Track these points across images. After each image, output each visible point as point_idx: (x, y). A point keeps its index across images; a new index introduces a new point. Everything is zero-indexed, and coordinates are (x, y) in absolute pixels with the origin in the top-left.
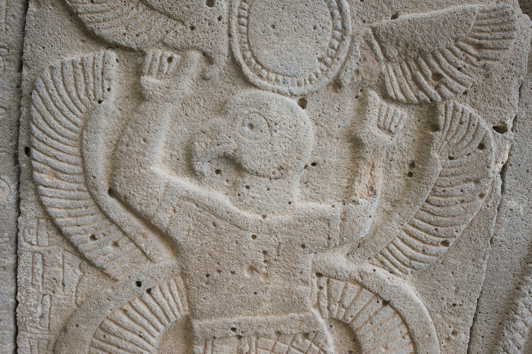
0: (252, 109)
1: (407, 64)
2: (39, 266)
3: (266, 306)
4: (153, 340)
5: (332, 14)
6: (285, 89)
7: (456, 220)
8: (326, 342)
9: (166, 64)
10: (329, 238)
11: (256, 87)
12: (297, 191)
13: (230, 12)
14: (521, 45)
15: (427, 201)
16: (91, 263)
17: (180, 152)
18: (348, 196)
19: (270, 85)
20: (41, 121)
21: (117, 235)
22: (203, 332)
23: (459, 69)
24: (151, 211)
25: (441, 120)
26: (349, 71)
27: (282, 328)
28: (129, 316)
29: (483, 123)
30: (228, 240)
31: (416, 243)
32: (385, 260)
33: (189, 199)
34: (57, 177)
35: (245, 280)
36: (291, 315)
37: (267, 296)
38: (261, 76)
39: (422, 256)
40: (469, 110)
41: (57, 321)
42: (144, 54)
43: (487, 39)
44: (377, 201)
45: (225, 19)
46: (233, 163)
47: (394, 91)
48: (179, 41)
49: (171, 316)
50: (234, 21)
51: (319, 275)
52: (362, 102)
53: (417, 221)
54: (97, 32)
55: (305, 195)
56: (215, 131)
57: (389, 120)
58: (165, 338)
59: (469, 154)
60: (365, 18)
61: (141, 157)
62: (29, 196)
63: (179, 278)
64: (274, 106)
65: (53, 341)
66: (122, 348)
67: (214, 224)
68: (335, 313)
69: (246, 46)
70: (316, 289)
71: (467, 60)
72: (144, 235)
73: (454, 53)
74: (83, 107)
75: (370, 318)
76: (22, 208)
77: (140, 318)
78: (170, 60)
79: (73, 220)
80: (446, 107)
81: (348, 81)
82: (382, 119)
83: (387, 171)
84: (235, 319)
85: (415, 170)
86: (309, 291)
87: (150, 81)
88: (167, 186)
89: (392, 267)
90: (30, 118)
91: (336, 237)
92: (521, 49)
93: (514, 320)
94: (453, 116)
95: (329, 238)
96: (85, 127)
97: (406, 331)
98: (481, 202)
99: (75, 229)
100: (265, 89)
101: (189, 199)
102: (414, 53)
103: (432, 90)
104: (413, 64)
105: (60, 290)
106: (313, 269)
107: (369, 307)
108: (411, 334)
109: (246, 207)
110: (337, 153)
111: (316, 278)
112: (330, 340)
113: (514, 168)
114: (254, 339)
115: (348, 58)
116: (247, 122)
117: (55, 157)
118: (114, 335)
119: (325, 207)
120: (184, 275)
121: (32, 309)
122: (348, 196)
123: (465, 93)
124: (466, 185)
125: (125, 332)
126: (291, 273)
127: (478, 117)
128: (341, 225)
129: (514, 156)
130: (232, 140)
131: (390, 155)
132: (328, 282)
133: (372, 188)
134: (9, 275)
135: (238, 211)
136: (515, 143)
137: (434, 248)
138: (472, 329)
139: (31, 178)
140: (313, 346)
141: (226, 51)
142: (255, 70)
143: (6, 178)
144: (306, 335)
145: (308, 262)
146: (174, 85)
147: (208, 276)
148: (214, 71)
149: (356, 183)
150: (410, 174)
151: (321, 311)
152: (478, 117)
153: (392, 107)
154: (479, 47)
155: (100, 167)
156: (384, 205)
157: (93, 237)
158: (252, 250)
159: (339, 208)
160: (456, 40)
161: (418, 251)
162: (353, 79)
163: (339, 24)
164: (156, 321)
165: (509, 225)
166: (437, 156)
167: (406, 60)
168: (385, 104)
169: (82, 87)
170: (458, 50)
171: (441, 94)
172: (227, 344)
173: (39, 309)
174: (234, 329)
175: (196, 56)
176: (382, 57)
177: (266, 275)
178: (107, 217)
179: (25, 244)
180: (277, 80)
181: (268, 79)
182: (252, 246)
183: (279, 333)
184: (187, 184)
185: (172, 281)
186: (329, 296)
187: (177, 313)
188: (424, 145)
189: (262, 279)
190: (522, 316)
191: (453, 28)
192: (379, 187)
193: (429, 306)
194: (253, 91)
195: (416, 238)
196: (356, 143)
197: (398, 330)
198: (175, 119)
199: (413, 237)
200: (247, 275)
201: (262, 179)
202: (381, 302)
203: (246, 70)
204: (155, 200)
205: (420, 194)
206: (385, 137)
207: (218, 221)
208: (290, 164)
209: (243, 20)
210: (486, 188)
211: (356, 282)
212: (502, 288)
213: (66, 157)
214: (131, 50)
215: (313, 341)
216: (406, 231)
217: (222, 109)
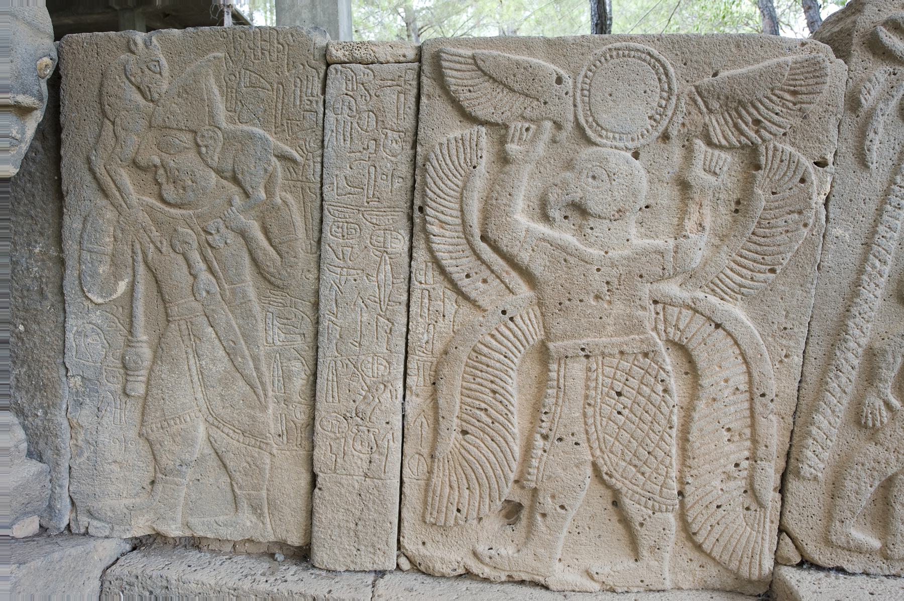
0: (594, 163)
1: (729, 114)
2: (426, 301)
3: (610, 329)
4: (515, 360)
5: (659, 79)
6: (621, 144)
7: (781, 249)
8: (664, 361)
9: (525, 134)
10: (664, 269)
11: (597, 145)
12: (633, 230)
13: (575, 87)
14: (836, 87)
15: (753, 233)
16: (466, 297)
17: (536, 203)
18: (679, 232)
19: (609, 143)
20: (433, 185)
21: (486, 273)
22: (557, 352)
23: (777, 114)
24: (515, 251)
25: (763, 160)
26: (676, 124)
27: (625, 348)
28: (496, 340)
29: (803, 159)
30: (577, 273)
31: (744, 271)
32: (716, 288)
33: (544, 240)
34: (442, 228)
35: (591, 306)
36: (632, 336)
37: (611, 321)
38: (601, 136)
39: (751, 283)
40: (789, 148)
41: (439, 346)
42: (506, 127)
43: (801, 86)
45: (571, 94)
46: (580, 209)
47: (717, 136)
48: (534, 115)
49: (530, 339)
50: (578, 94)
51: (656, 302)
52: (689, 150)
53: (745, 252)
54: (473, 114)
55: (641, 233)
56: (565, 184)
57: (713, 164)
58: (523, 361)
59: (790, 189)
60: (688, 78)
61: (507, 208)
62: (420, 244)
63: (536, 308)
64: (613, 160)
65: (435, 363)
66: (492, 367)
67: (565, 260)
68: (671, 335)
69: (589, 113)
70: (654, 315)
71: (783, 105)
72: (507, 273)
73: (771, 101)
74: (462, 172)
75: (704, 340)
76: (414, 255)
77: (506, 341)
78: (527, 129)
79: (454, 262)
80: (766, 148)
81: (676, 133)
82: (707, 163)
83: (715, 209)
84: (584, 341)
85: (740, 207)
86: (648, 316)
87: (513, 148)
88: (527, 231)
89: (723, 294)
90: (425, 184)
91: (669, 267)
92: (836, 90)
93: (845, 341)
94: (774, 156)
95: (664, 269)
96: (464, 187)
97: (738, 352)
98: (805, 232)
99: (456, 269)
100: (604, 146)
101: (544, 240)
102: (735, 103)
103: (752, 134)
104: (734, 113)
105: (441, 319)
106: (650, 296)
107: (702, 329)
108: (743, 355)
109: (591, 245)
110: (668, 196)
111: (652, 307)
112: (668, 360)
113: (837, 198)
114: (600, 358)
115: (674, 114)
116: (591, 174)
117: (442, 213)
118: (485, 356)
119: (659, 243)
120: (540, 304)
121: (420, 336)
122: (679, 232)
123: (785, 134)
124: (790, 216)
125: (493, 353)
126: (631, 299)
127: (798, 155)
128: (674, 257)
129: (837, 187)
130: (579, 190)
131: (717, 195)
132: (664, 309)
133: (700, 225)
134: (403, 308)
135: (584, 248)
136: (837, 176)
137: (762, 275)
138: (804, 352)
139: (424, 230)
140: (653, 364)
141: (572, 118)
142: (595, 131)
143: (402, 232)
144: (646, 355)
145: (646, 290)
146: (531, 151)
147: (560, 304)
148: (563, 136)
149: (686, 221)
150: (736, 211)
151: (658, 334)
152: (798, 155)
153: (717, 152)
154: (794, 93)
155: (475, 218)
156: (712, 240)
157: (468, 276)
158: (597, 282)
159: (672, 242)
160: (772, 90)
161: (746, 279)
162: (679, 131)
163: (666, 86)
164: (518, 344)
165: (836, 252)
166: (760, 192)
167: (727, 111)
168: (710, 150)
169: (462, 157)
170: (774, 98)
171: (761, 137)
172: (577, 363)
173: (425, 335)
174: (583, 349)
175: (548, 125)
176: (705, 110)
177: (610, 302)
178: (479, 258)
179: (416, 283)
180: (614, 138)
181: (607, 138)
182: (597, 278)
183: (622, 353)
184: (542, 228)
185: (530, 310)
186: (665, 320)
187: (535, 337)
188: (748, 185)
189: (606, 306)
190: (853, 336)
191: (769, 79)
192: (707, 224)
193: (761, 330)
194: (595, 149)
195: (745, 267)
196: (684, 186)
197: (731, 351)
198: (531, 176)
199: (741, 266)
200: (594, 303)
201: (604, 221)
202: (713, 325)
203: (589, 132)
204: (518, 242)
205: (745, 227)
206: (711, 179)
207: (568, 258)
208: (627, 207)
209: (586, 93)
210: (809, 218)
211: (689, 307)
212: (832, 312)
213: (449, 212)
214: (498, 124)
215: (653, 360)
216: (734, 261)
217: (569, 165)
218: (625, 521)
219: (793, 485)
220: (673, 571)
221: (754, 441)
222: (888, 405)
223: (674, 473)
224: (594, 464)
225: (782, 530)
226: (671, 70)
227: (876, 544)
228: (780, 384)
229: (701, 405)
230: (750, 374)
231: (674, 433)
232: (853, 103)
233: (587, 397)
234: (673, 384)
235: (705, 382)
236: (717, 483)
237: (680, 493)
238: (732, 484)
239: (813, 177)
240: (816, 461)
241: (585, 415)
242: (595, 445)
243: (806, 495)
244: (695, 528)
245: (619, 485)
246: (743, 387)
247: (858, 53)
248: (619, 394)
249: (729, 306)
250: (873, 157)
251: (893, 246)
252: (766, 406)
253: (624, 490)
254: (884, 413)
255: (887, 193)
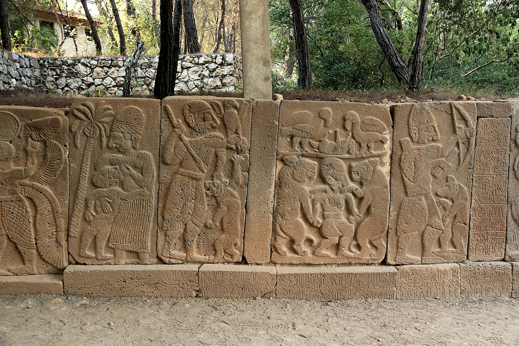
27: (12, 199)
44: (35, 166)
85: (45, 157)
102: (37, 128)
103: (44, 138)
110: (22, 154)
111: (20, 187)
112: (26, 202)
119: (20, 168)
122: (26, 165)
144: (19, 201)
153: (35, 142)
154: (53, 127)
177: (6, 185)
188: (45, 151)
205: (46, 163)
218: (20, 253)
219: (70, 239)
220: (37, 269)
221: (57, 226)
222: (92, 214)
223: (33, 238)
224: (7, 235)
225: (69, 253)
226: (17, 119)
227: (94, 255)
228: (62, 209)
229: (38, 216)
230: (51, 206)
231: (31, 224)
232: (70, 130)
233: (2, 214)
234: (29, 210)
235: (38, 209)
236: (47, 239)
237: (36, 244)
238: (51, 240)
239: (62, 150)
240: (75, 231)
241: (2, 220)
242: (6, 229)
243: (74, 242)
244: (42, 254)
245: (15, 241)
246: (51, 210)
247: (71, 115)
248: (12, 213)
249: (43, 186)
250: (79, 145)
251: (88, 169)
252: (58, 215)
253: (17, 243)
254: (91, 217)
255: (84, 154)
